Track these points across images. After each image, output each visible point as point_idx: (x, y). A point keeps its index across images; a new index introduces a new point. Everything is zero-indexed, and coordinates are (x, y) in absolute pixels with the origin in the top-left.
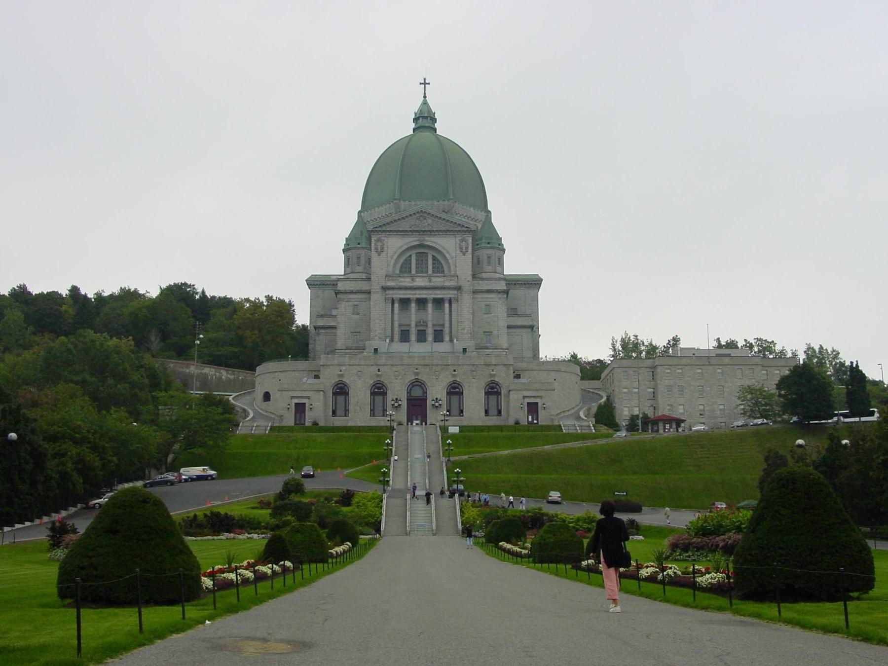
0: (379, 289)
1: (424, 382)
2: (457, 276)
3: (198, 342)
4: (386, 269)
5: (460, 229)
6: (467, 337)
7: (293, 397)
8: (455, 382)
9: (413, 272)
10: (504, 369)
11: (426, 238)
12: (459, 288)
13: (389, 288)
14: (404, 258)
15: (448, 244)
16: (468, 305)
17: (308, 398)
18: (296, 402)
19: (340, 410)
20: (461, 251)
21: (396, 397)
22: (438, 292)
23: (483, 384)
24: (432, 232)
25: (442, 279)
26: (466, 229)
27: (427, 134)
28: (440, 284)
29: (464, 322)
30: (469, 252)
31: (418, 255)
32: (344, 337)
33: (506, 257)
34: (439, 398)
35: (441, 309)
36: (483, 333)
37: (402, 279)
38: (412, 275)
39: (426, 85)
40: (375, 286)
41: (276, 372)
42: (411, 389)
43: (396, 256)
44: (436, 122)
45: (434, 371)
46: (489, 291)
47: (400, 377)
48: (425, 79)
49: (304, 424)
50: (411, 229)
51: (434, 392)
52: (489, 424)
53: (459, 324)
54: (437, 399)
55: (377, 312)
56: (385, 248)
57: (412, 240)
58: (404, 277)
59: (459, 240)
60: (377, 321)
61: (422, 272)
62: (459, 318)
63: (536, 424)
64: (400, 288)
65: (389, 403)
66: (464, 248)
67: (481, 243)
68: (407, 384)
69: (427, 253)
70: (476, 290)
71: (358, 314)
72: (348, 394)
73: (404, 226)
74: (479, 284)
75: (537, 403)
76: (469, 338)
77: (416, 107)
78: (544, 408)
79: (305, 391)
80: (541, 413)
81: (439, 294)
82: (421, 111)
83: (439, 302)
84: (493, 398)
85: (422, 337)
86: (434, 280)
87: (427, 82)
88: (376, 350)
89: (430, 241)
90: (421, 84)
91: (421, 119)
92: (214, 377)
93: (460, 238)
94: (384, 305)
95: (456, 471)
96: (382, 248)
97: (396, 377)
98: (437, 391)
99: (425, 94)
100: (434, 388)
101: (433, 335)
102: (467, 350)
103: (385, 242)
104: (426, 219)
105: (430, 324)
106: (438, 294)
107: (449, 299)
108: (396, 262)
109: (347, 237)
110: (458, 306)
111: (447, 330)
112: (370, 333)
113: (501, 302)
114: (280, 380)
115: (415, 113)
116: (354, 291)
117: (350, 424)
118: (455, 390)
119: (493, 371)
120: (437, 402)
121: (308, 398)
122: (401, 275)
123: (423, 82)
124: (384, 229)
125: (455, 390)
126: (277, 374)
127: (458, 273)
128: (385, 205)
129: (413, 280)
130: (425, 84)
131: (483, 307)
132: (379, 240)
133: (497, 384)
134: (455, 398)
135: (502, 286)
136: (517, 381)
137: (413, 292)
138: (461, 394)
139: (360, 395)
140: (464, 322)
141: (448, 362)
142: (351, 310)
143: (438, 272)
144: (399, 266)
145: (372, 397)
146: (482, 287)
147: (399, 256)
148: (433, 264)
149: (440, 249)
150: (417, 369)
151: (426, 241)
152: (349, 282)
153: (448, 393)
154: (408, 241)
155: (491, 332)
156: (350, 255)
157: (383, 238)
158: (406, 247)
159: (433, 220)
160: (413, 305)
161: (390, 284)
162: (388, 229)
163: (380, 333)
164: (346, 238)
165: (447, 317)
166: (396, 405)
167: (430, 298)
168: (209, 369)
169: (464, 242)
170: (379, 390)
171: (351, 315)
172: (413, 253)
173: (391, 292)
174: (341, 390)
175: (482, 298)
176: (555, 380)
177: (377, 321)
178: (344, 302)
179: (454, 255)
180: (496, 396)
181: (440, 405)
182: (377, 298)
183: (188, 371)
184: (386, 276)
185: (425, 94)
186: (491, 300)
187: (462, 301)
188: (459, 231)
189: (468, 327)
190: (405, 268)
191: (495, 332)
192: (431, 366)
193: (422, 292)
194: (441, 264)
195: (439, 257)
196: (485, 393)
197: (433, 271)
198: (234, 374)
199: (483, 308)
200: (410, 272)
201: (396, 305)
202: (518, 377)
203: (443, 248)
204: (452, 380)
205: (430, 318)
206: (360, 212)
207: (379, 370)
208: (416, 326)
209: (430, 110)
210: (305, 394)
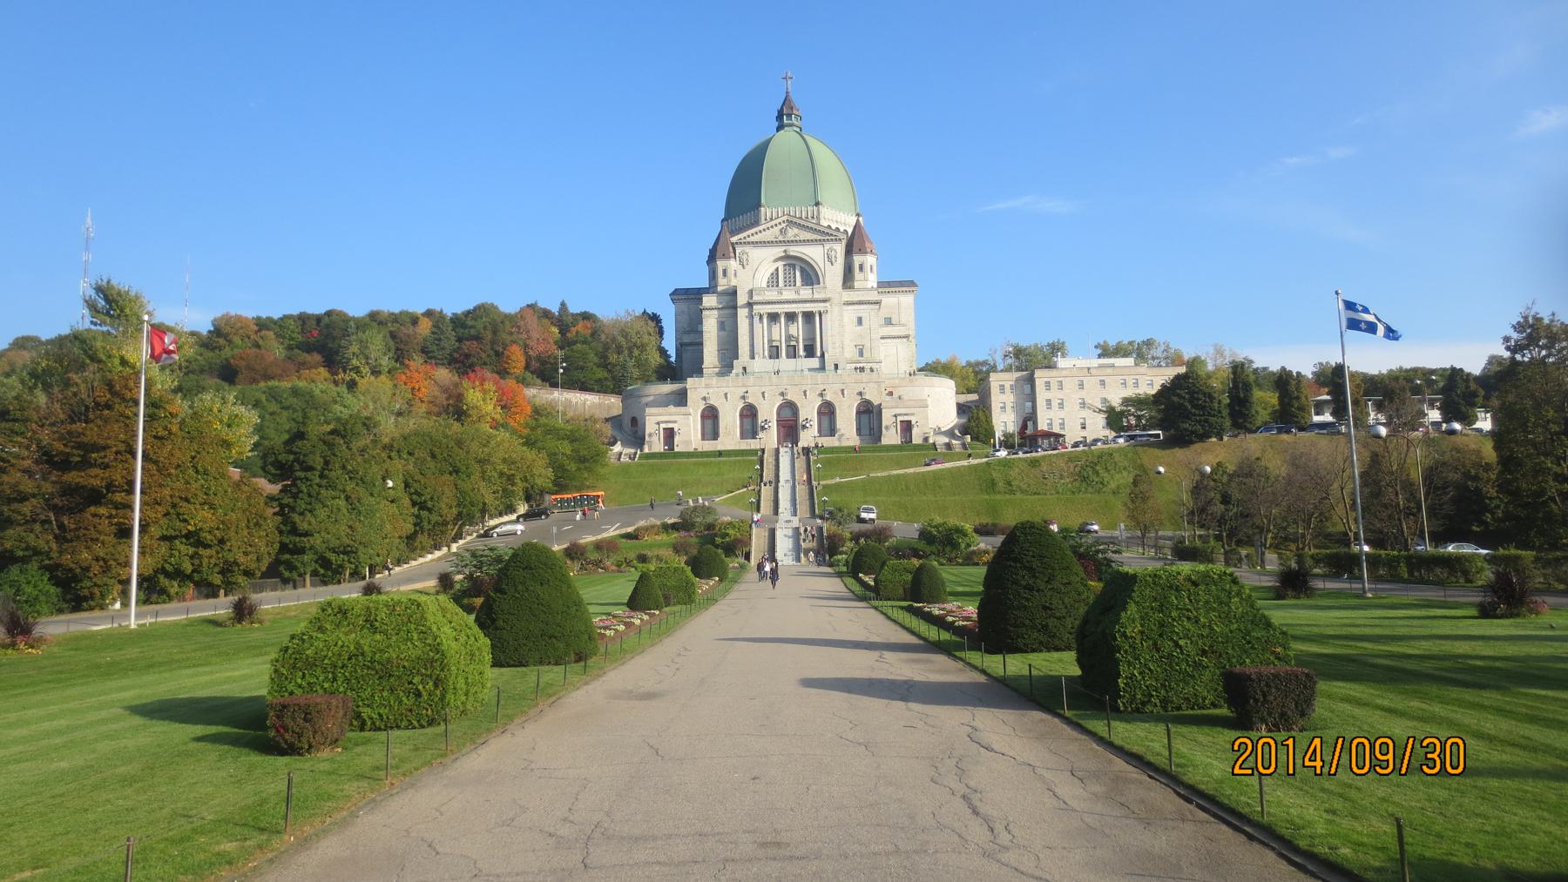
13: (757, 303)
14: (772, 270)
22: (807, 305)
26: (833, 238)
35: (810, 323)
46: (860, 303)
49: (673, 450)
57: (778, 251)
83: (809, 316)
85: (792, 353)
88: (745, 369)
91: (785, 117)
98: (809, 412)
105: (801, 340)
117: (720, 448)
118: (827, 412)
121: (675, 422)
123: (784, 76)
124: (748, 240)
125: (827, 412)
131: (855, 320)
132: (743, 253)
135: (874, 296)
136: (888, 398)
139: (730, 421)
153: (820, 413)
170: (749, 413)
172: (780, 264)
174: (711, 416)
179: (822, 266)
186: (862, 311)
190: (774, 280)
193: (790, 306)
201: (765, 320)
202: (891, 394)
204: (819, 402)
206: (723, 221)
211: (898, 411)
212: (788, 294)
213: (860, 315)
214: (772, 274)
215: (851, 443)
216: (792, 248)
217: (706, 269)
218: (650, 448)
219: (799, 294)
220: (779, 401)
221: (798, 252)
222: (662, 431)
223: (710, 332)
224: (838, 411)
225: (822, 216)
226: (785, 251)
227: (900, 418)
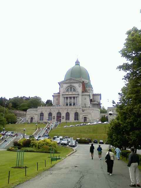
7: (30, 116)
12: (78, 94)
14: (67, 88)
15: (76, 85)
17: (34, 116)
23: (74, 113)
27: (78, 66)
40: (61, 95)
46: (86, 95)
73: (67, 82)
75: (86, 117)
77: (76, 61)
80: (87, 119)
81: (74, 96)
83: (74, 98)
85: (70, 105)
89: (73, 85)
97: (54, 112)
98: (64, 114)
105: (72, 102)
118: (68, 115)
121: (34, 116)
125: (68, 115)
129: (69, 93)
132: (62, 85)
139: (46, 116)
144: (66, 90)
147: (66, 88)
158: (67, 86)
160: (69, 98)
165: (76, 101)
170: (50, 114)
174: (42, 115)
190: (67, 91)
195: (75, 88)
201: (65, 98)
204: (67, 112)
208: (69, 102)
209: (78, 61)
210: (33, 115)
211: (84, 115)
216: (72, 84)
217: (59, 90)
220: (57, 112)
224: (70, 114)
227: (84, 116)
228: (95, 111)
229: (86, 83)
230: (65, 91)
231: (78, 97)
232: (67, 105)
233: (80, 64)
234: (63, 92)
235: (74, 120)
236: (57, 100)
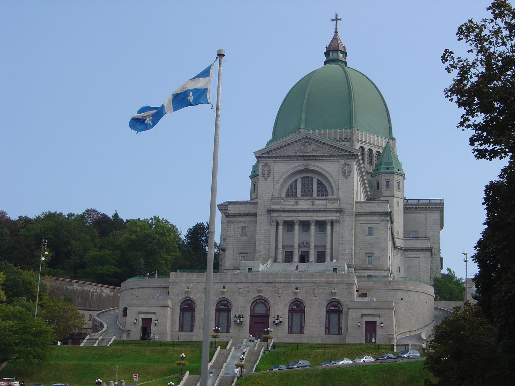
0: (265, 212)
1: (267, 299)
2: (339, 199)
3: (43, 259)
4: (272, 193)
5: (343, 153)
6: (348, 259)
8: (297, 300)
9: (299, 194)
10: (346, 287)
11: (312, 164)
12: (340, 211)
13: (273, 211)
14: (290, 182)
16: (349, 227)
17: (154, 313)
18: (143, 317)
19: (187, 326)
20: (343, 175)
21: (240, 314)
22: (321, 214)
24: (315, 157)
25: (324, 202)
28: (322, 207)
29: (346, 243)
30: (351, 176)
31: (304, 179)
32: (232, 257)
33: (406, 184)
34: (280, 315)
35: (323, 231)
36: (364, 255)
37: (286, 203)
38: (296, 199)
39: (339, 22)
40: (261, 210)
41: (133, 289)
42: (254, 306)
43: (282, 180)
44: (346, 55)
45: (276, 289)
46: (371, 214)
47: (244, 295)
48: (336, 15)
50: (296, 155)
51: (276, 310)
52: (329, 342)
53: (340, 246)
54: (278, 316)
55: (262, 233)
56: (272, 173)
57: (297, 165)
58: (288, 200)
59: (342, 164)
60: (262, 242)
61: (307, 196)
62: (340, 239)
63: (373, 342)
64: (284, 211)
65: (233, 319)
66: (347, 173)
67: (380, 169)
68: (250, 301)
69: (312, 178)
70: (359, 212)
71: (247, 236)
72: (194, 310)
73: (290, 151)
74: (362, 206)
76: (349, 260)
78: (382, 327)
79: (151, 306)
80: (379, 332)
81: (321, 217)
82: (330, 45)
83: (321, 225)
84: (334, 317)
85: (304, 258)
86: (317, 202)
87: (339, 18)
89: (315, 165)
90: (333, 20)
91: (331, 53)
92: (95, 294)
93: (343, 163)
94: (269, 227)
95: (169, 384)
96: (269, 173)
99: (336, 29)
100: (276, 306)
101: (310, 254)
102: (338, 269)
103: (271, 168)
104: (311, 145)
105: (312, 245)
106: (321, 216)
107: (331, 221)
108: (282, 186)
109: (254, 165)
110: (339, 228)
111: (328, 252)
112: (255, 254)
113: (383, 224)
114: (137, 296)
115: (326, 48)
116: (242, 214)
119: (334, 289)
120: (278, 319)
121: (154, 313)
122: (286, 199)
123: (334, 18)
124: (271, 155)
126: (134, 291)
127: (341, 196)
128: (292, 134)
129: (297, 203)
130: (336, 19)
131: (366, 229)
132: (266, 165)
133: (338, 303)
134: (296, 317)
137: (296, 215)
138: (302, 311)
140: (346, 243)
141: (291, 280)
142: (240, 232)
143: (323, 196)
144: (285, 190)
145: (217, 313)
146: (365, 209)
147: (285, 181)
148: (318, 188)
149: (324, 173)
150: (260, 287)
151: (308, 165)
152: (238, 206)
153: (290, 311)
154: (293, 166)
155: (373, 254)
156: (256, 181)
157: (270, 164)
158: (292, 171)
159: (317, 146)
160: (297, 227)
161: (275, 207)
162: (274, 155)
163: (265, 254)
164: (253, 165)
165: (329, 238)
166: (238, 321)
167: (312, 220)
168: (90, 286)
169: (347, 166)
171: (240, 236)
172: (299, 177)
173: (275, 215)
175: (366, 220)
176: (402, 299)
177: (262, 242)
178: (233, 225)
179: (336, 178)
180: (300, 314)
181: (281, 322)
182: (262, 220)
183: (71, 288)
184: (272, 200)
185: (336, 29)
186: (372, 222)
187: (344, 223)
188: (342, 155)
189: (349, 248)
190: (291, 192)
191: (377, 254)
192: (274, 284)
193: (305, 214)
194: (326, 188)
195: (323, 181)
196: (326, 311)
197: (317, 194)
198: (113, 292)
199: (366, 230)
200: (296, 195)
201: (281, 227)
202: (364, 295)
203: (327, 172)
204: (292, 297)
205: (312, 239)
207: (224, 287)
208: (299, 246)
210: (152, 310)
212: (304, 205)
213: (371, 225)
214: (291, 186)
215: (320, 341)
216: (311, 163)
217: (248, 182)
218: (129, 335)
219: (313, 204)
221: (315, 166)
222: (140, 320)
223: (232, 236)
225: (355, 138)
226: (304, 165)
228: (412, 294)
229: (374, 150)
230: (280, 191)
231: (338, 221)
232: (288, 257)
233: (347, 59)
234: (270, 196)
235: (323, 330)
236: (244, 234)
